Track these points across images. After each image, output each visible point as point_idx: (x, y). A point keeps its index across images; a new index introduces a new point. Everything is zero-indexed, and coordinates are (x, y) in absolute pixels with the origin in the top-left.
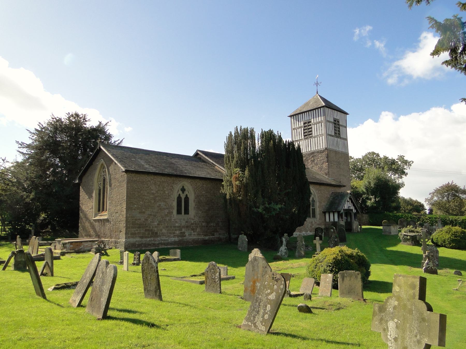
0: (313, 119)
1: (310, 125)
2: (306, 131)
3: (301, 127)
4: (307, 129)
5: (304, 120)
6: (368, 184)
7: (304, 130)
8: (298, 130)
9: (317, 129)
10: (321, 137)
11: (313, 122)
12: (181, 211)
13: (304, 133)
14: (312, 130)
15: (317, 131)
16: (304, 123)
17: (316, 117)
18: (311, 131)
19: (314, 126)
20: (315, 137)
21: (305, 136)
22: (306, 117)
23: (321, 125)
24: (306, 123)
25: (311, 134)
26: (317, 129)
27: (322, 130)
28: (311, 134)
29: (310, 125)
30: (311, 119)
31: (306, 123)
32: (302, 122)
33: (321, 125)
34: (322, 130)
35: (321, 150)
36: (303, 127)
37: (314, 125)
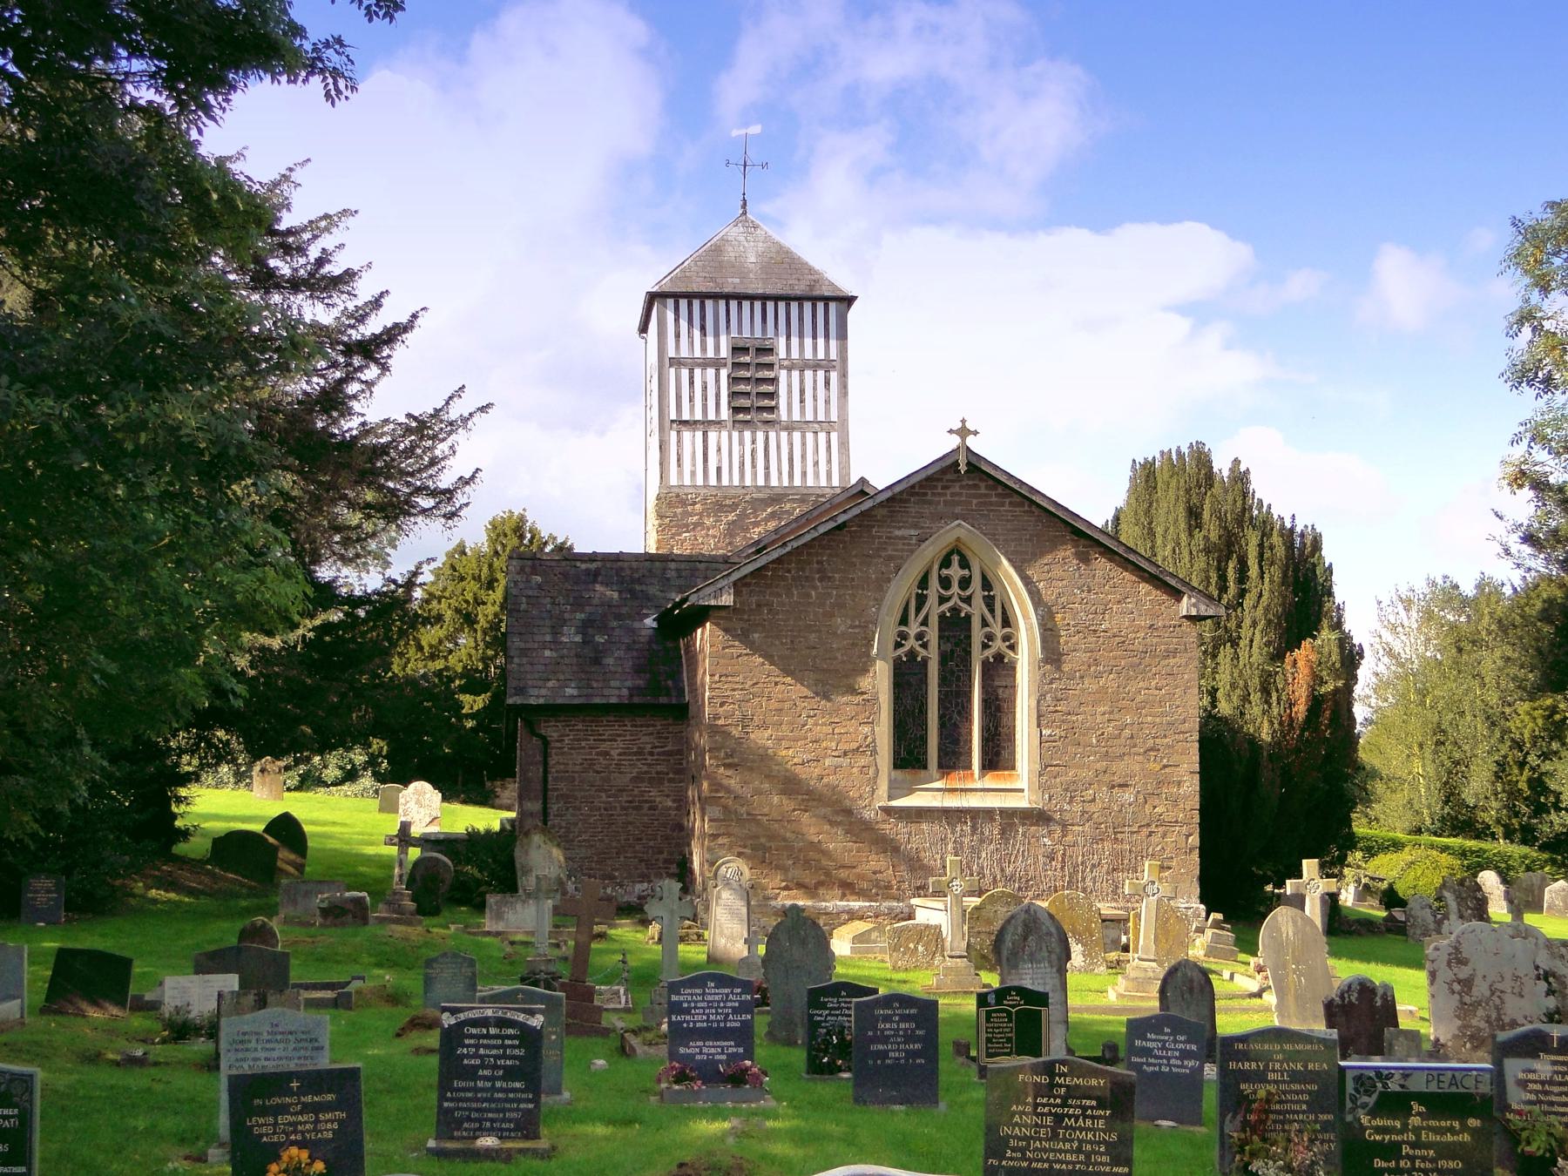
0: (782, 340)
1: (770, 366)
2: (742, 387)
3: (717, 364)
4: (748, 379)
5: (734, 334)
6: (1374, 679)
7: (734, 380)
8: (698, 372)
9: (802, 392)
10: (822, 436)
11: (782, 355)
12: (925, 753)
13: (733, 395)
14: (778, 403)
15: (802, 401)
16: (737, 350)
17: (801, 336)
18: (772, 395)
19: (789, 376)
20: (793, 429)
21: (736, 410)
22: (748, 325)
23: (827, 383)
24: (745, 350)
25: (771, 409)
26: (802, 392)
27: (827, 402)
28: (771, 409)
29: (770, 366)
30: (777, 334)
31: (745, 350)
32: (723, 339)
33: (827, 383)
34: (827, 402)
35: (819, 492)
36: (730, 365)
37: (789, 369)
